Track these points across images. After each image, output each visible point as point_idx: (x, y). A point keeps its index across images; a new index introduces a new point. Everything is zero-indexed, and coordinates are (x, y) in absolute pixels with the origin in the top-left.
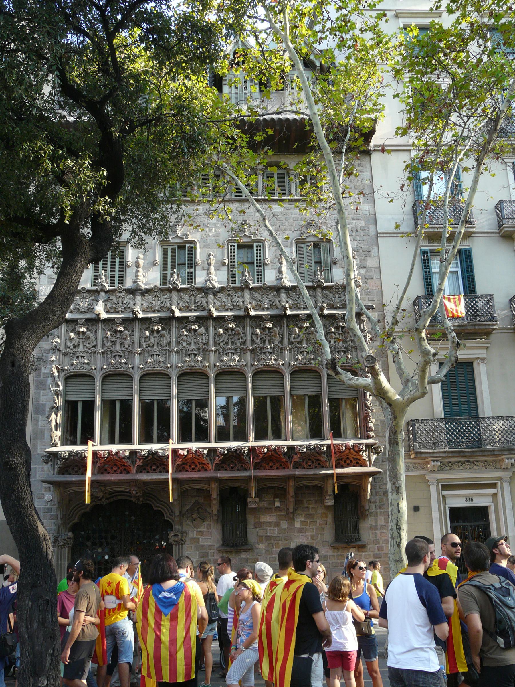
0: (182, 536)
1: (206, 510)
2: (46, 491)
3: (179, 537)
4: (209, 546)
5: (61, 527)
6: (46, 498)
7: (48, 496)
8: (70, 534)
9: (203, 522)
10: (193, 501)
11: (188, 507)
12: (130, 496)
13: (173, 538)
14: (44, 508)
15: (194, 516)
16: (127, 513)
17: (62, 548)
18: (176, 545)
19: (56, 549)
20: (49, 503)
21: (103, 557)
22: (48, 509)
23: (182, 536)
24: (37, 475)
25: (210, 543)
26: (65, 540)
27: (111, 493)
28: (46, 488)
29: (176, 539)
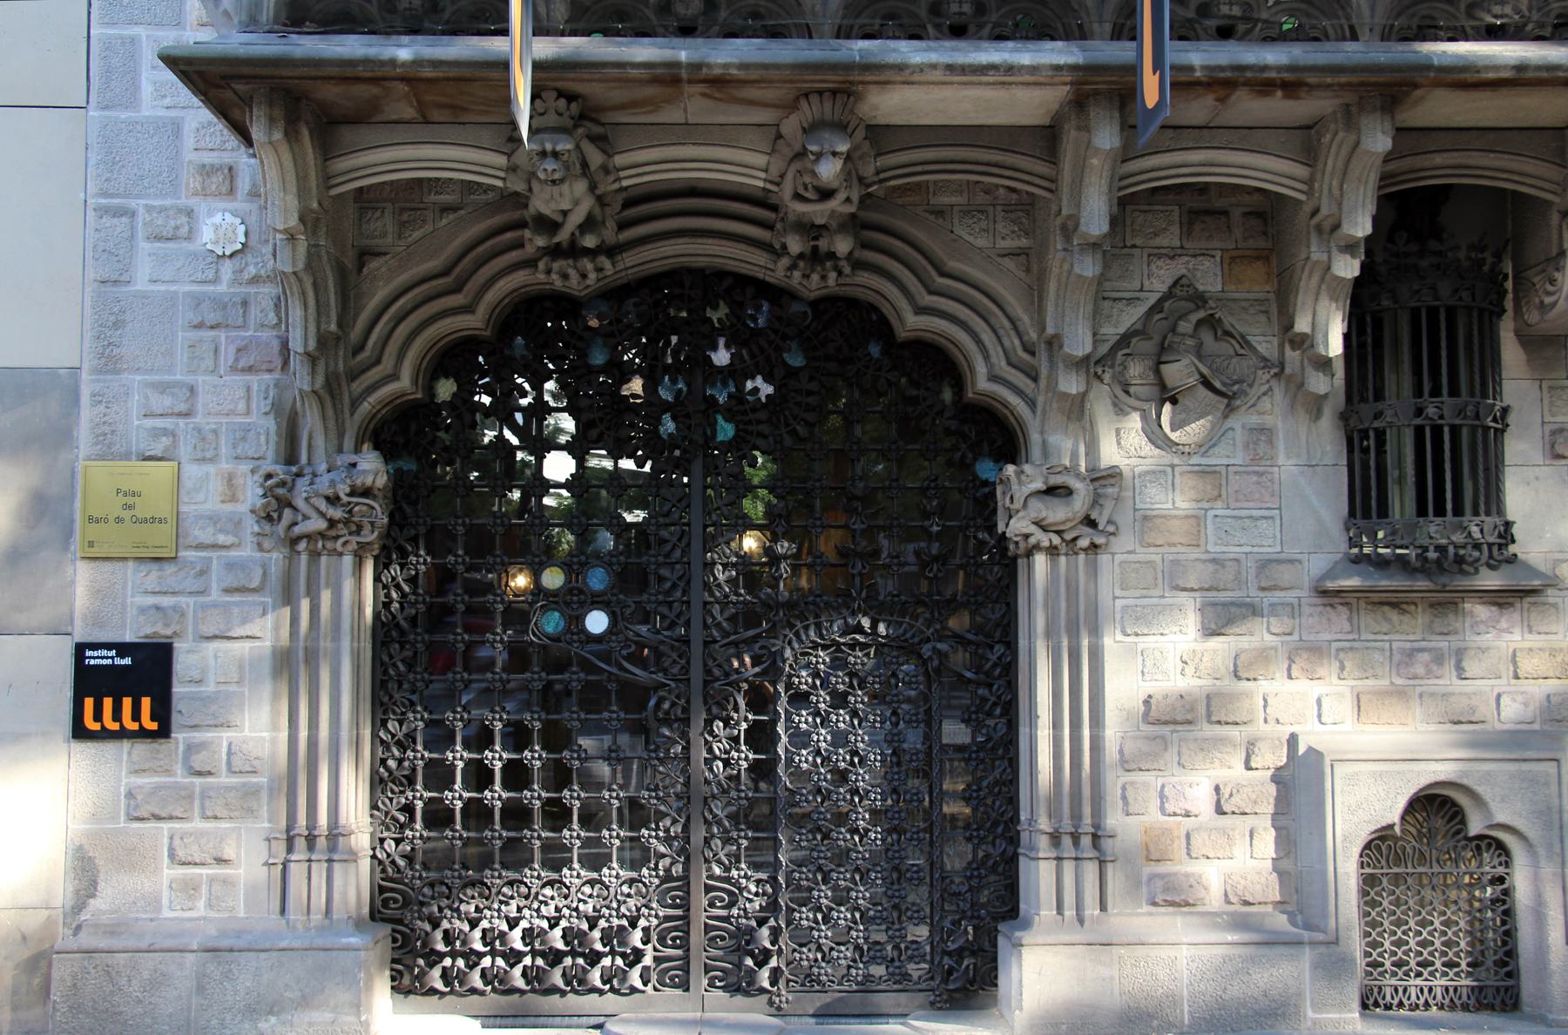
0: (1096, 501)
1: (1244, 342)
2: (204, 193)
3: (1079, 504)
4: (1265, 564)
5: (311, 421)
6: (207, 235)
7: (220, 226)
8: (372, 467)
9: (1230, 410)
10: (1159, 279)
11: (1129, 317)
12: (769, 226)
13: (1039, 508)
14: (197, 301)
15: (1179, 372)
16: (721, 357)
17: (315, 555)
18: (1052, 551)
19: (277, 557)
20: (227, 268)
21: (576, 622)
22: (220, 304)
23: (1096, 501)
24: (147, 89)
25: (1270, 549)
26: (333, 500)
27: (642, 202)
28: (206, 171)
29: (1057, 512)
